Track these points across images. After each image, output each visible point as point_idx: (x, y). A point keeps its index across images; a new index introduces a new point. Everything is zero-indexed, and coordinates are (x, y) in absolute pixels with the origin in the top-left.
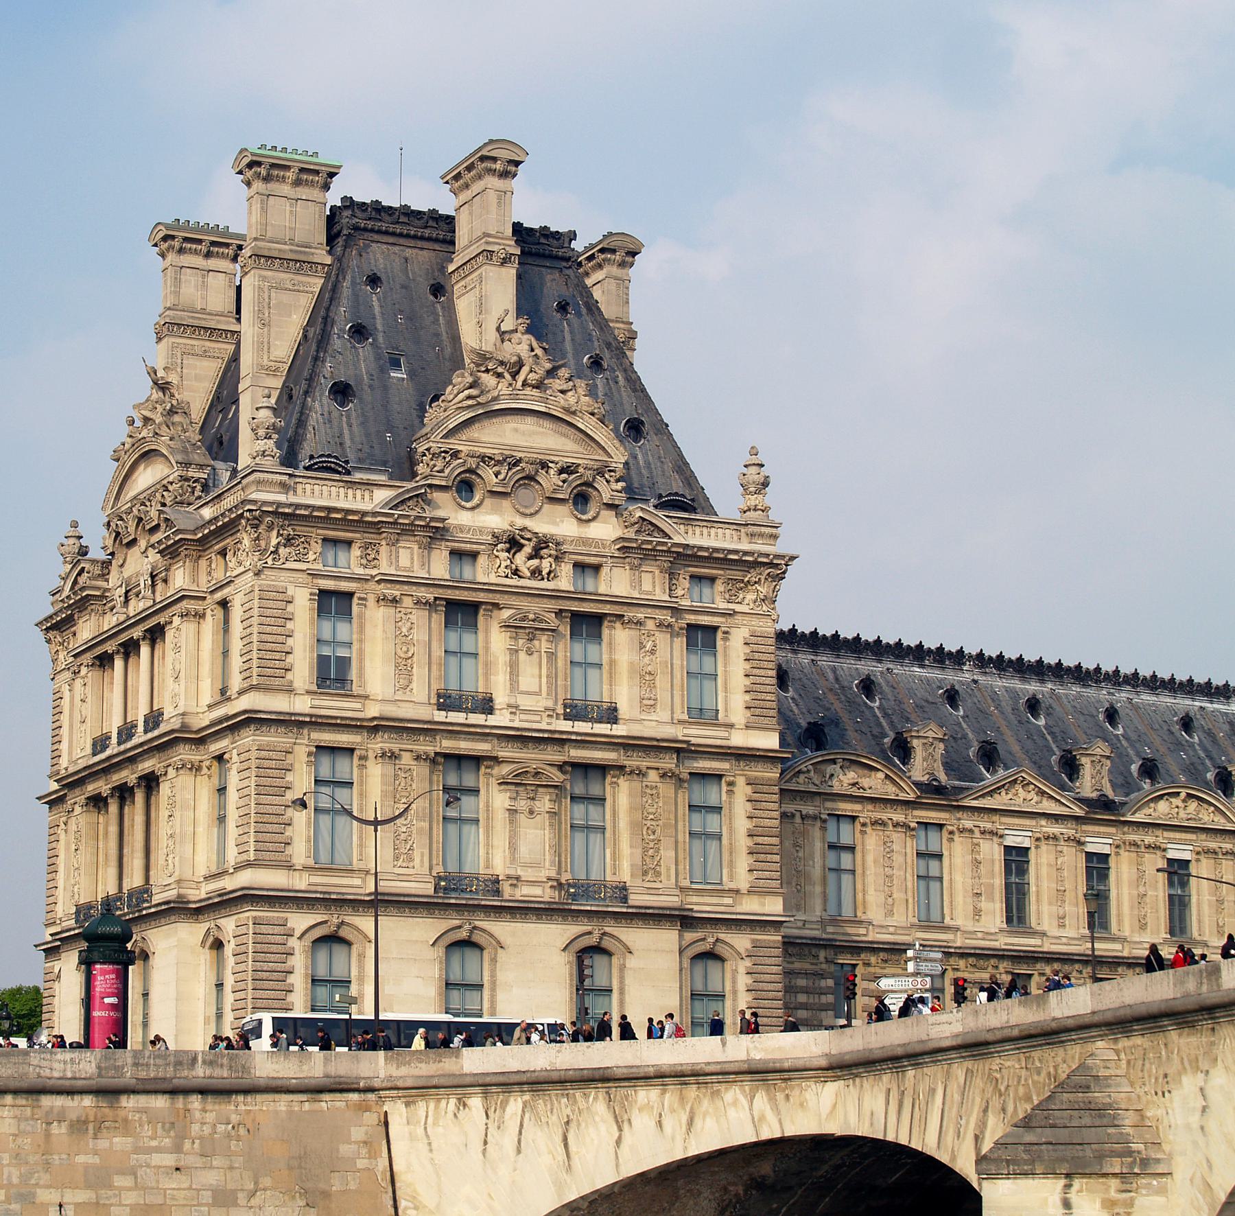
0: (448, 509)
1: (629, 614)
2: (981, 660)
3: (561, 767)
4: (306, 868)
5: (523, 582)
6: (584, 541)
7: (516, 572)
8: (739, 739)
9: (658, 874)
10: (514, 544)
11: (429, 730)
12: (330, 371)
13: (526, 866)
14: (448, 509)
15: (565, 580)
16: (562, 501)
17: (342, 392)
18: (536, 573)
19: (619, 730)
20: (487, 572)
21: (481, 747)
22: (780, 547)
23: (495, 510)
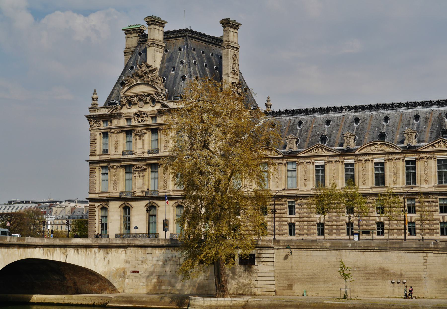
1: (160, 127)
2: (349, 109)
4: (98, 193)
5: (139, 124)
6: (153, 111)
7: (139, 122)
9: (167, 187)
11: (119, 161)
13: (138, 188)
15: (149, 121)
16: (148, 103)
20: (133, 123)
21: (130, 163)
23: (135, 108)
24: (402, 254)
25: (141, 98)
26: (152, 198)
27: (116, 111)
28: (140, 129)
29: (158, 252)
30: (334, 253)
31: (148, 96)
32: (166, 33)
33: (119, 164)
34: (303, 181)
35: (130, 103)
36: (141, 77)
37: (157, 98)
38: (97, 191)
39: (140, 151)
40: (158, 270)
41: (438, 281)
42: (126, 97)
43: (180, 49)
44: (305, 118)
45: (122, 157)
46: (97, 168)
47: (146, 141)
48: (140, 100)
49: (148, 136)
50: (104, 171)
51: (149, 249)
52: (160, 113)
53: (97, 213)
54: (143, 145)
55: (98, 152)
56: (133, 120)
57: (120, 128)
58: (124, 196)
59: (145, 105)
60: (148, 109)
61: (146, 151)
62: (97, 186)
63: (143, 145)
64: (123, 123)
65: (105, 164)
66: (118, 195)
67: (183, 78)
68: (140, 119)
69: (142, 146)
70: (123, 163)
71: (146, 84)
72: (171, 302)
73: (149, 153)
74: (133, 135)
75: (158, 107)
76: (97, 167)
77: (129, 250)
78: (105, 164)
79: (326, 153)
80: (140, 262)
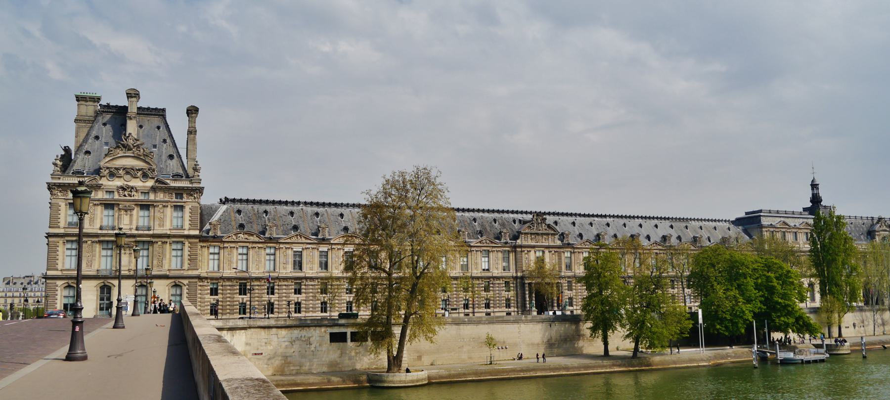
0: (104, 182)
2: (306, 203)
3: (135, 242)
8: (186, 233)
10: (124, 189)
11: (97, 235)
12: (87, 147)
14: (104, 182)
15: (138, 197)
17: (88, 153)
18: (130, 196)
19: (151, 232)
20: (116, 196)
22: (201, 185)
24: (504, 326)
25: (129, 171)
26: (142, 277)
27: (94, 182)
28: (128, 204)
29: (283, 332)
30: (454, 327)
31: (139, 170)
32: (139, 108)
33: (97, 239)
34: (282, 265)
35: (112, 175)
36: (130, 149)
37: (149, 173)
38: (60, 267)
39: (128, 227)
40: (281, 350)
41: (528, 345)
42: (108, 168)
43: (159, 128)
44: (269, 208)
45: (100, 232)
46: (61, 242)
47: (135, 217)
48: (127, 173)
49: (136, 211)
50: (69, 246)
51: (274, 330)
52: (154, 189)
53: (59, 293)
54: (131, 221)
55: (62, 224)
56: (116, 193)
57: (99, 200)
58: (104, 273)
59: (134, 180)
60: (137, 183)
61: (134, 227)
62: (60, 262)
63: (131, 221)
64: (100, 195)
65: (74, 238)
66: (94, 273)
67: (171, 157)
68: (126, 193)
69: (131, 222)
70: (102, 239)
71: (137, 157)
72: (344, 381)
73: (137, 229)
74: (116, 209)
75: (150, 183)
76: (61, 241)
77: (249, 331)
78: (74, 238)
79: (304, 240)
80: (263, 344)
